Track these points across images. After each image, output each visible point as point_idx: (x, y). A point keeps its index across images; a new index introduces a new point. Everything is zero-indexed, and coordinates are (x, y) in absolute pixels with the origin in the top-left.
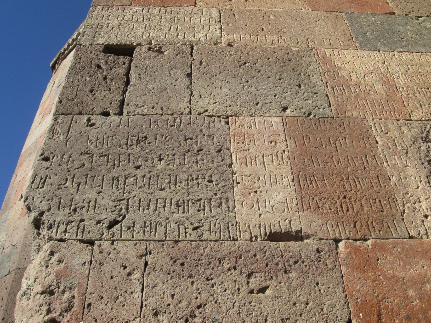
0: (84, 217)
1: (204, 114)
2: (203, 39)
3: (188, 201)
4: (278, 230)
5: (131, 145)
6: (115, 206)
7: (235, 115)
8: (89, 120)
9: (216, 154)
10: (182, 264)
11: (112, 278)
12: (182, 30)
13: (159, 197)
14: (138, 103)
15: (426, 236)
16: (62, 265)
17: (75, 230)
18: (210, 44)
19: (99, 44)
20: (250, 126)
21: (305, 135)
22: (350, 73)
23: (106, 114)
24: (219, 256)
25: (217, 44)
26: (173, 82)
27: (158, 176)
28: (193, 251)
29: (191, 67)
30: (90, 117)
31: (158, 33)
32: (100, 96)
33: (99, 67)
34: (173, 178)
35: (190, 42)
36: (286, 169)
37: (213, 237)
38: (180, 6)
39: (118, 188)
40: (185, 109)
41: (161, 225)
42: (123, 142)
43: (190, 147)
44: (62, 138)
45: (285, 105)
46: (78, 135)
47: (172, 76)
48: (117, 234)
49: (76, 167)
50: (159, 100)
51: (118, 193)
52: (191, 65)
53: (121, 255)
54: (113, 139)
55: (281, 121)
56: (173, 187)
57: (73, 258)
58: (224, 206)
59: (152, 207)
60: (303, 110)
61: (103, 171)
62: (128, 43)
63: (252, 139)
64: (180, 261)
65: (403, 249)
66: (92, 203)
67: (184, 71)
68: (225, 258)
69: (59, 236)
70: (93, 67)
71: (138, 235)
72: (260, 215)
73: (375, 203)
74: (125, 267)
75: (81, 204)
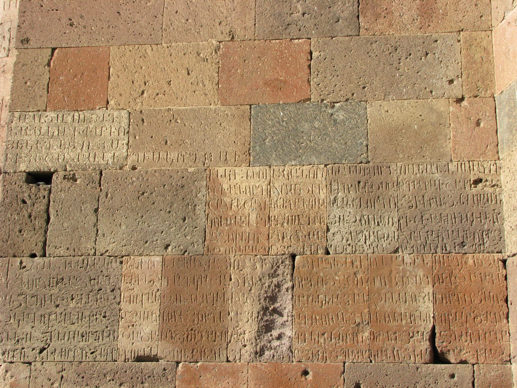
0: (24, 346)
1: (105, 254)
2: (110, 162)
3: (89, 333)
4: (143, 355)
5: (53, 286)
6: (43, 338)
7: (128, 255)
8: (21, 263)
9: (110, 293)
10: (83, 377)
11: (42, 386)
12: (93, 149)
13: (70, 330)
14: (56, 244)
15: (239, 361)
16: (13, 379)
17: (19, 356)
18: (116, 169)
19: (21, 172)
20: (137, 266)
21: (176, 274)
22: (232, 201)
23: (33, 256)
24: (105, 372)
25: (123, 167)
26: (83, 220)
27: (71, 313)
28: (89, 369)
29: (98, 200)
30: (21, 260)
31: (71, 154)
32: (27, 236)
33: (24, 202)
34: (80, 314)
35: (99, 166)
36: (155, 307)
37: (102, 359)
38: (92, 110)
39: (44, 323)
40: (91, 250)
41: (71, 350)
42: (47, 283)
43: (94, 287)
44: (3, 280)
45: (168, 243)
46: (15, 278)
47: (83, 211)
48: (45, 357)
49: (16, 307)
50: (72, 241)
51: (44, 327)
52: (99, 197)
53: (48, 371)
54: (39, 281)
55: (161, 261)
56: (80, 322)
57: (20, 375)
58: (111, 336)
59: (66, 338)
60: (181, 247)
61: (34, 310)
62: (46, 170)
63: (137, 279)
64: (82, 375)
65: (219, 370)
66: (29, 336)
67: (93, 206)
68: (108, 373)
69: (9, 360)
70: (20, 203)
71: (58, 358)
72: (133, 343)
73: (212, 334)
74: (50, 380)
75: (21, 337)
